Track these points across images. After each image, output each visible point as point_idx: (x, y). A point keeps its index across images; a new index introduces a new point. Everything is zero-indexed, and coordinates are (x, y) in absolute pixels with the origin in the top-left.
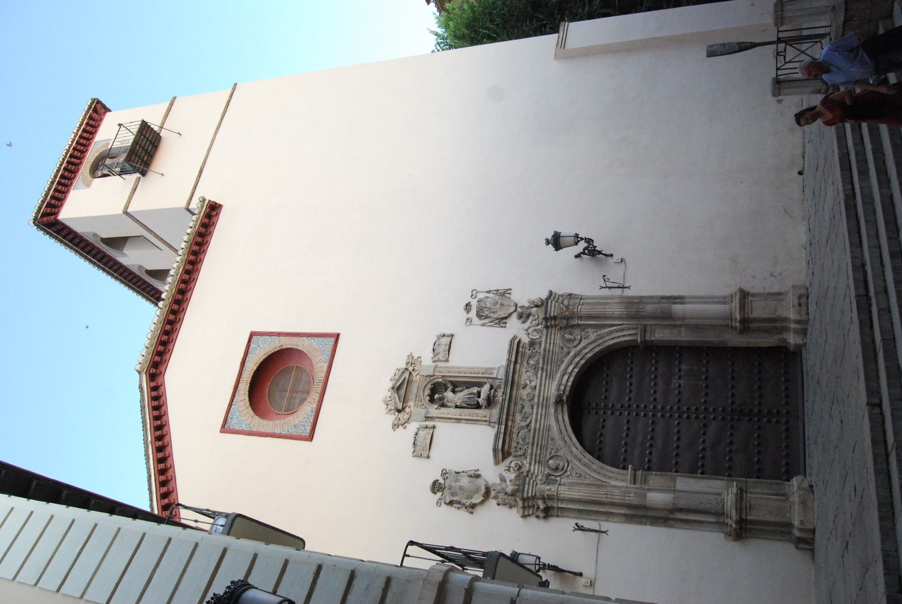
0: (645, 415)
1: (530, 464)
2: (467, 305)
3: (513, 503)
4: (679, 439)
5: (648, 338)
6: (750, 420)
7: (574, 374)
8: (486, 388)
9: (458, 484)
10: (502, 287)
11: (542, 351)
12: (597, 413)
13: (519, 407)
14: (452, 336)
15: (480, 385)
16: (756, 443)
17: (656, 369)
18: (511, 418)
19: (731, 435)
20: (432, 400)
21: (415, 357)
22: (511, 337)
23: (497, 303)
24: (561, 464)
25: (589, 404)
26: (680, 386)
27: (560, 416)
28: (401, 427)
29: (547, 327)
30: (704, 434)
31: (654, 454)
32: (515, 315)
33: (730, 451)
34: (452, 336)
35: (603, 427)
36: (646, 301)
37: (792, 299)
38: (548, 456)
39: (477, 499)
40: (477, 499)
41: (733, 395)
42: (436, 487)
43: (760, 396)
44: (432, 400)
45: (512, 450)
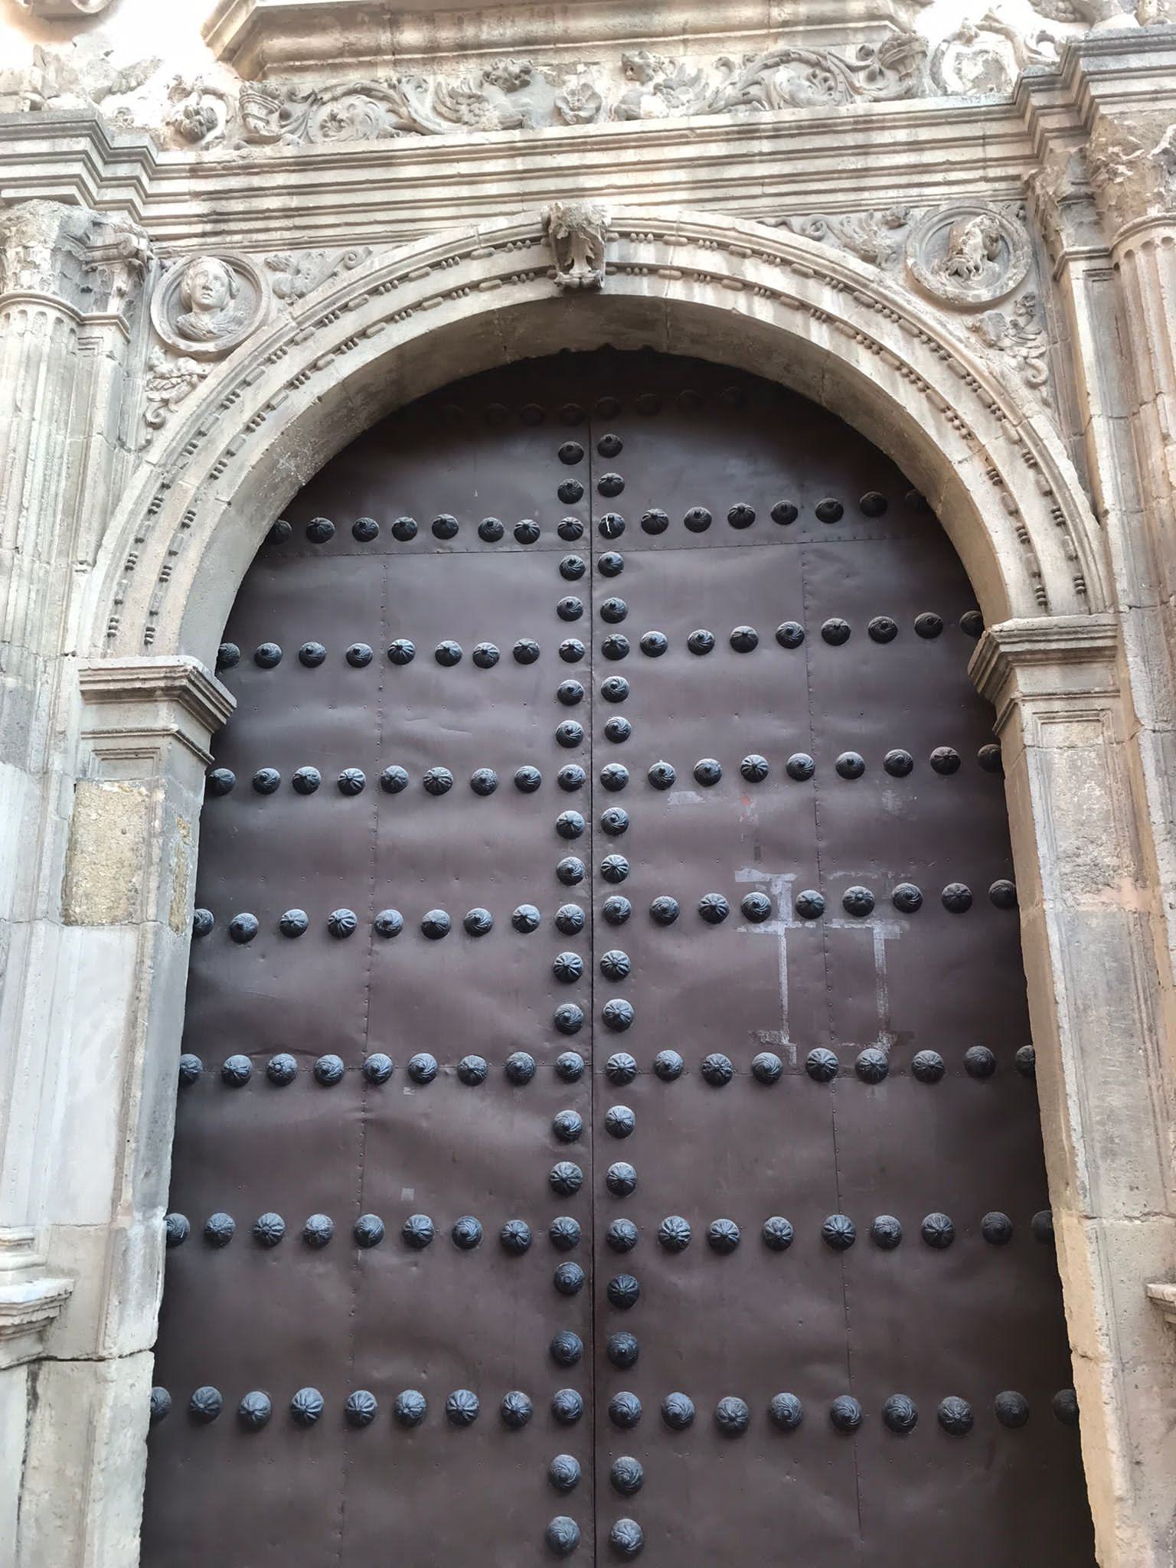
0: (567, 741)
1: (196, 171)
4: (433, 932)
5: (1024, 681)
6: (560, 1360)
7: (739, 303)
12: (569, 495)
16: (412, 1399)
17: (850, 772)
19: (463, 1243)
24: (205, 322)
25: (611, 451)
26: (755, 915)
27: (474, 271)
29: (1014, 109)
30: (469, 1079)
31: (347, 804)
33: (364, 1240)
35: (489, 535)
41: (721, 1247)
43: (729, 1431)
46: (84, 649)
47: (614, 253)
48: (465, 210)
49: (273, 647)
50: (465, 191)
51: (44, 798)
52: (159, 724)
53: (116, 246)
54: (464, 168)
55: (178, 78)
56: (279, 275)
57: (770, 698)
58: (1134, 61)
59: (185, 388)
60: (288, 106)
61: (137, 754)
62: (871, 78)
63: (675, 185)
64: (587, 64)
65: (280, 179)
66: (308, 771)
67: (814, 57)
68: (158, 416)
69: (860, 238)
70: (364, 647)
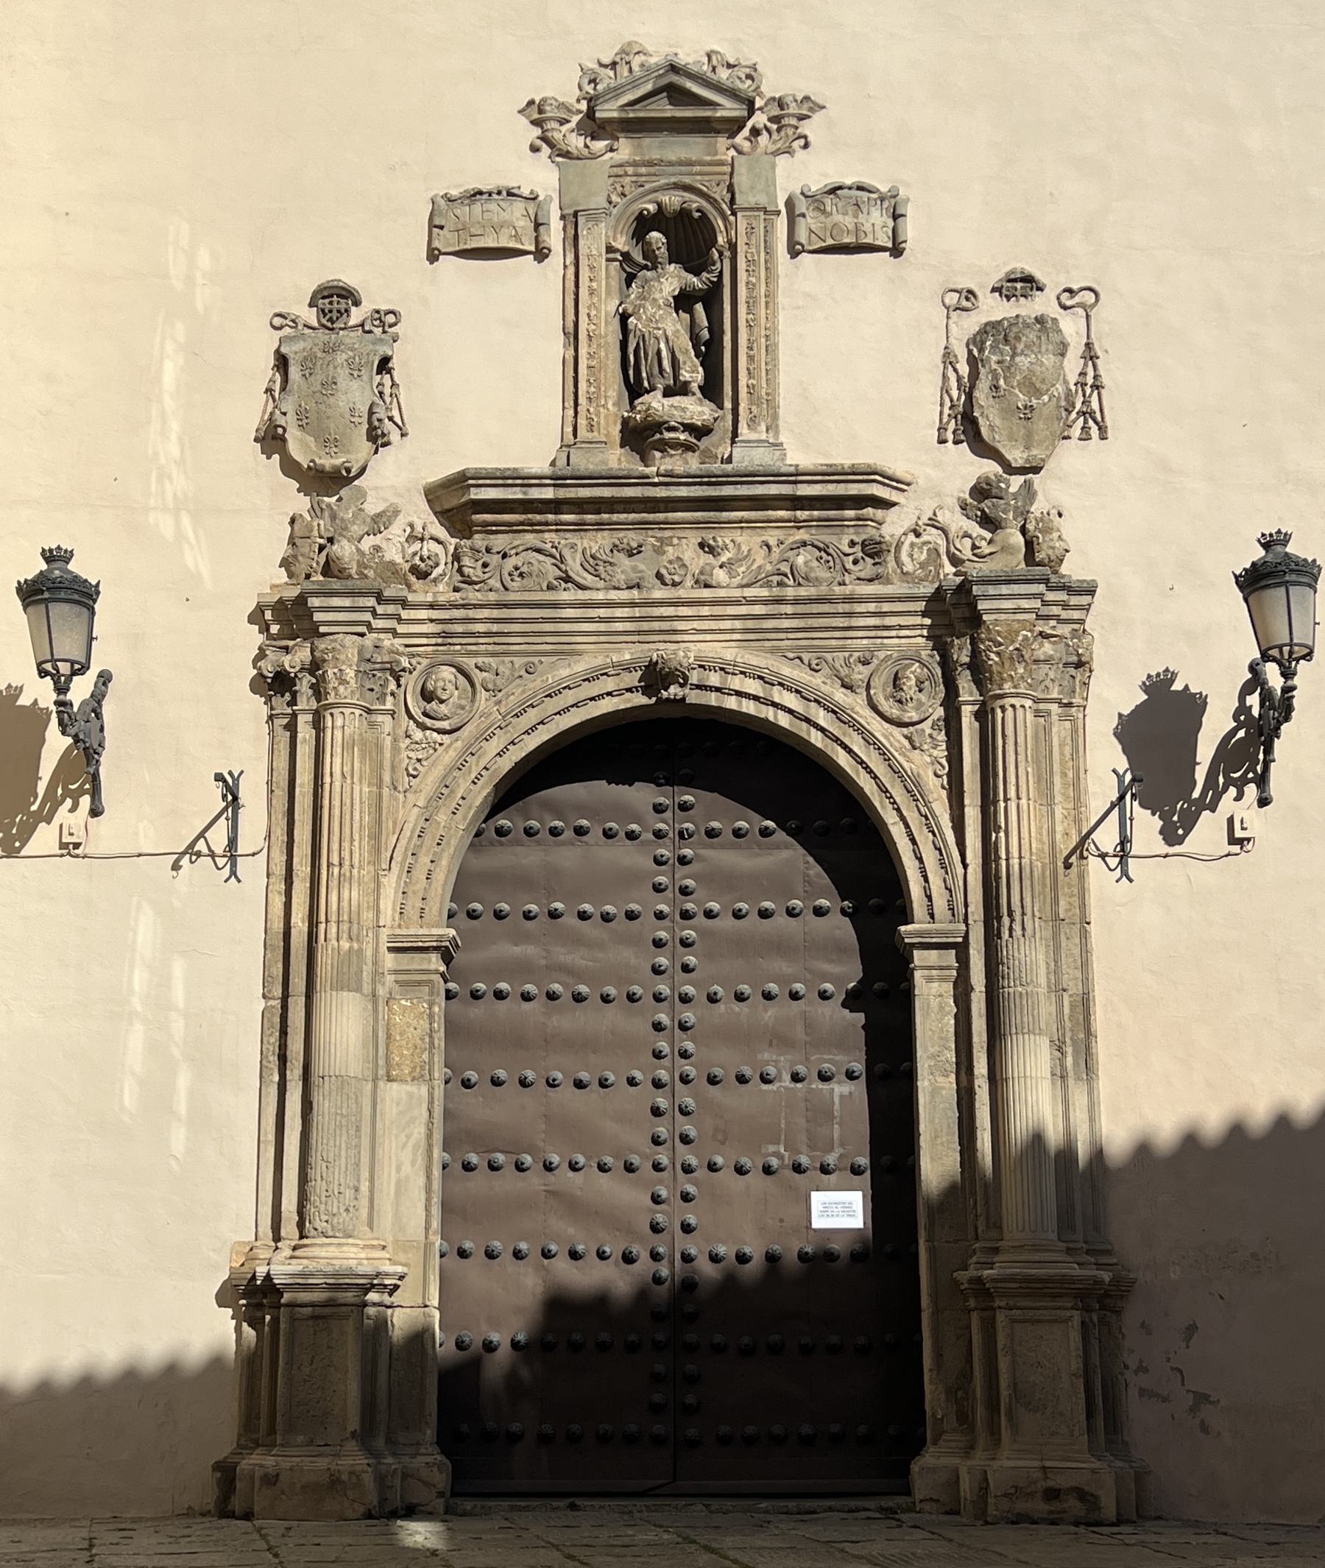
1: (432, 606)
2: (1028, 279)
3: (301, 568)
5: (917, 955)
8: (695, 409)
9: (342, 374)
10: (1114, 405)
11: (847, 590)
13: (632, 538)
14: (896, 250)
15: (711, 391)
18: (589, 517)
20: (643, 225)
21: (806, 128)
22: (899, 469)
23: (1038, 393)
24: (443, 709)
27: (610, 684)
28: (538, 132)
29: (938, 595)
31: (526, 1006)
32: (990, 468)
34: (896, 250)
35: (609, 834)
36: (1070, 946)
37: (1080, 1465)
38: (469, 663)
39: (300, 448)
40: (300, 448)
42: (334, 299)
44: (643, 225)
45: (479, 540)
46: (389, 924)
47: (694, 678)
48: (602, 639)
49: (477, 906)
50: (602, 627)
51: (375, 1010)
52: (433, 967)
53: (390, 663)
54: (602, 612)
55: (412, 526)
56: (485, 674)
57: (780, 947)
58: (1005, 589)
59: (431, 751)
60: (487, 558)
61: (419, 983)
62: (855, 562)
63: (732, 631)
64: (679, 538)
65: (486, 613)
66: (503, 986)
67: (822, 546)
68: (415, 769)
69: (844, 672)
70: (533, 907)
